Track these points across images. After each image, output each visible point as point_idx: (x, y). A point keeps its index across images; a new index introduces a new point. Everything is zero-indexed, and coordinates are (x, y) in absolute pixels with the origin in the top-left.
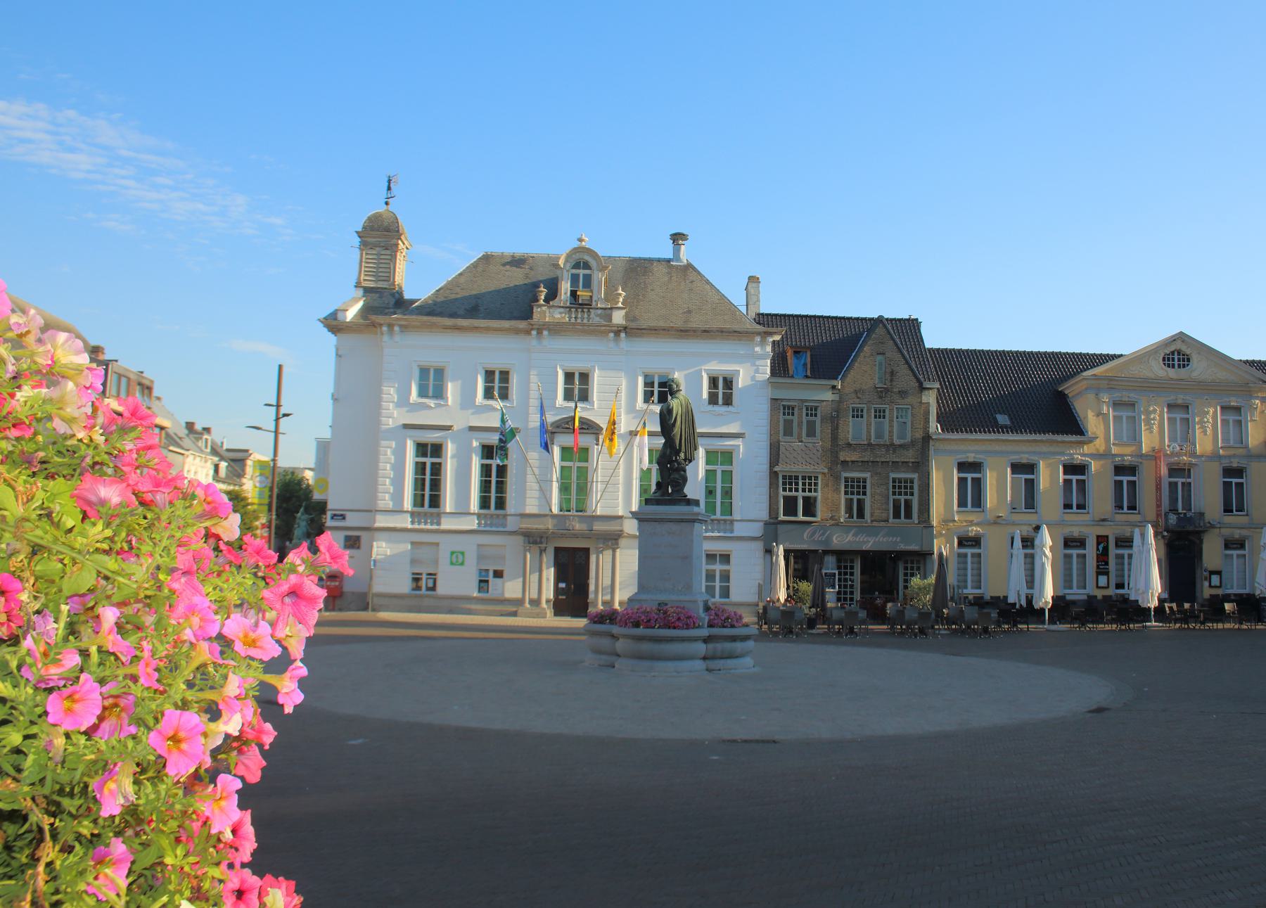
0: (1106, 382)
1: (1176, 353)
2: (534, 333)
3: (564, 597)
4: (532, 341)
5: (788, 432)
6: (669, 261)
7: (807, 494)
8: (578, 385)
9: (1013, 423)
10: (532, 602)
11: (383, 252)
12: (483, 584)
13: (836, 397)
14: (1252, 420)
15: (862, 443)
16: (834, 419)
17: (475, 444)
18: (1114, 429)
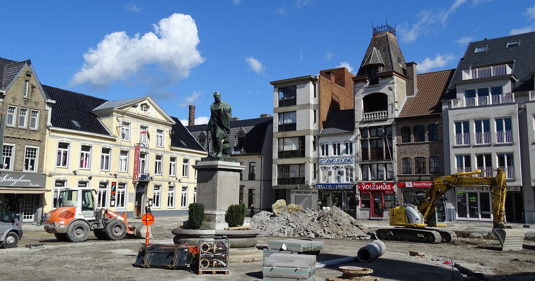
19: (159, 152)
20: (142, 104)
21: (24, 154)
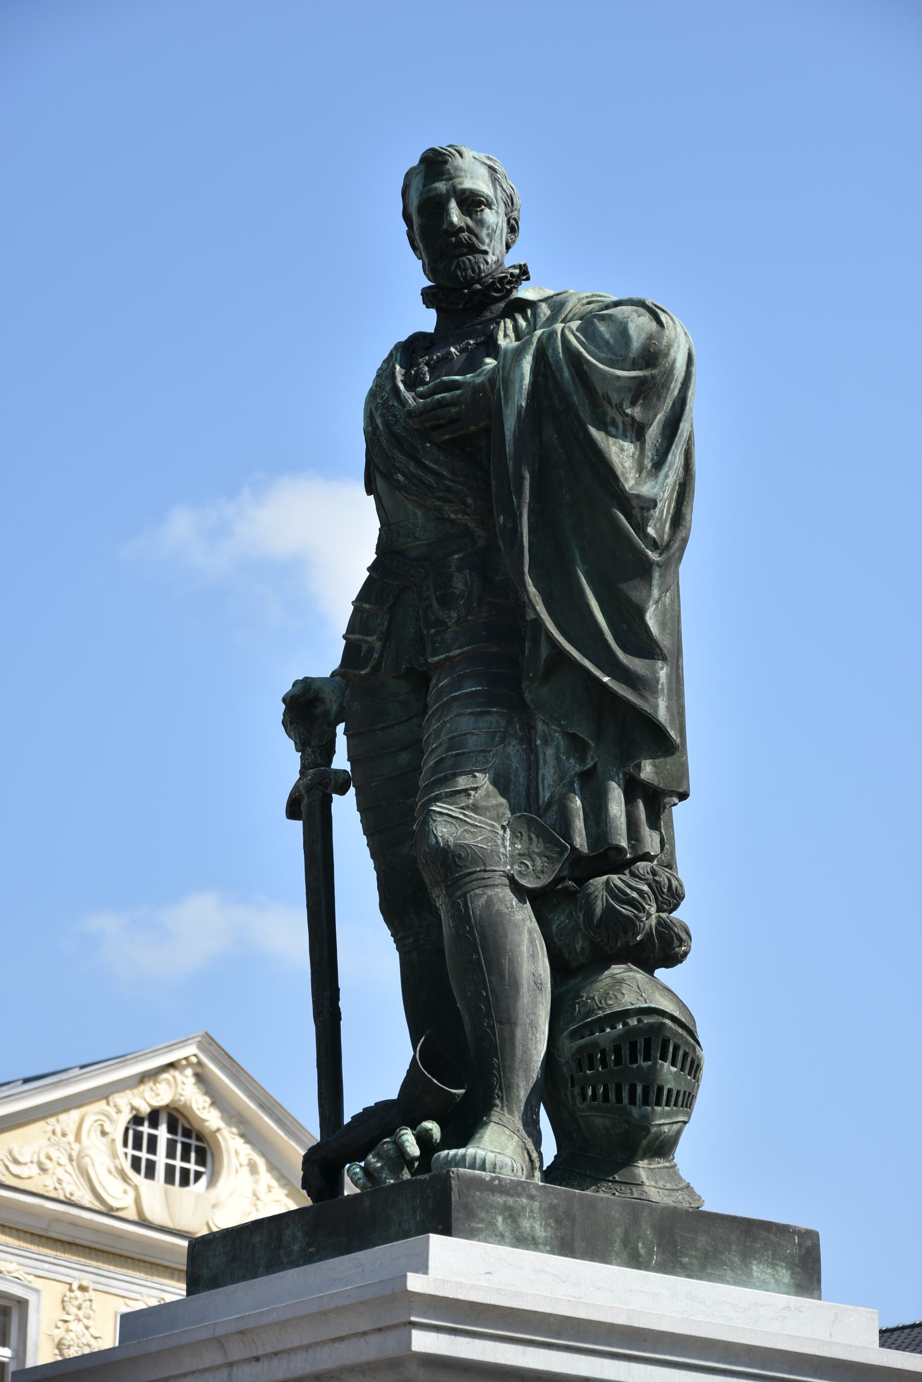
20: (137, 1120)
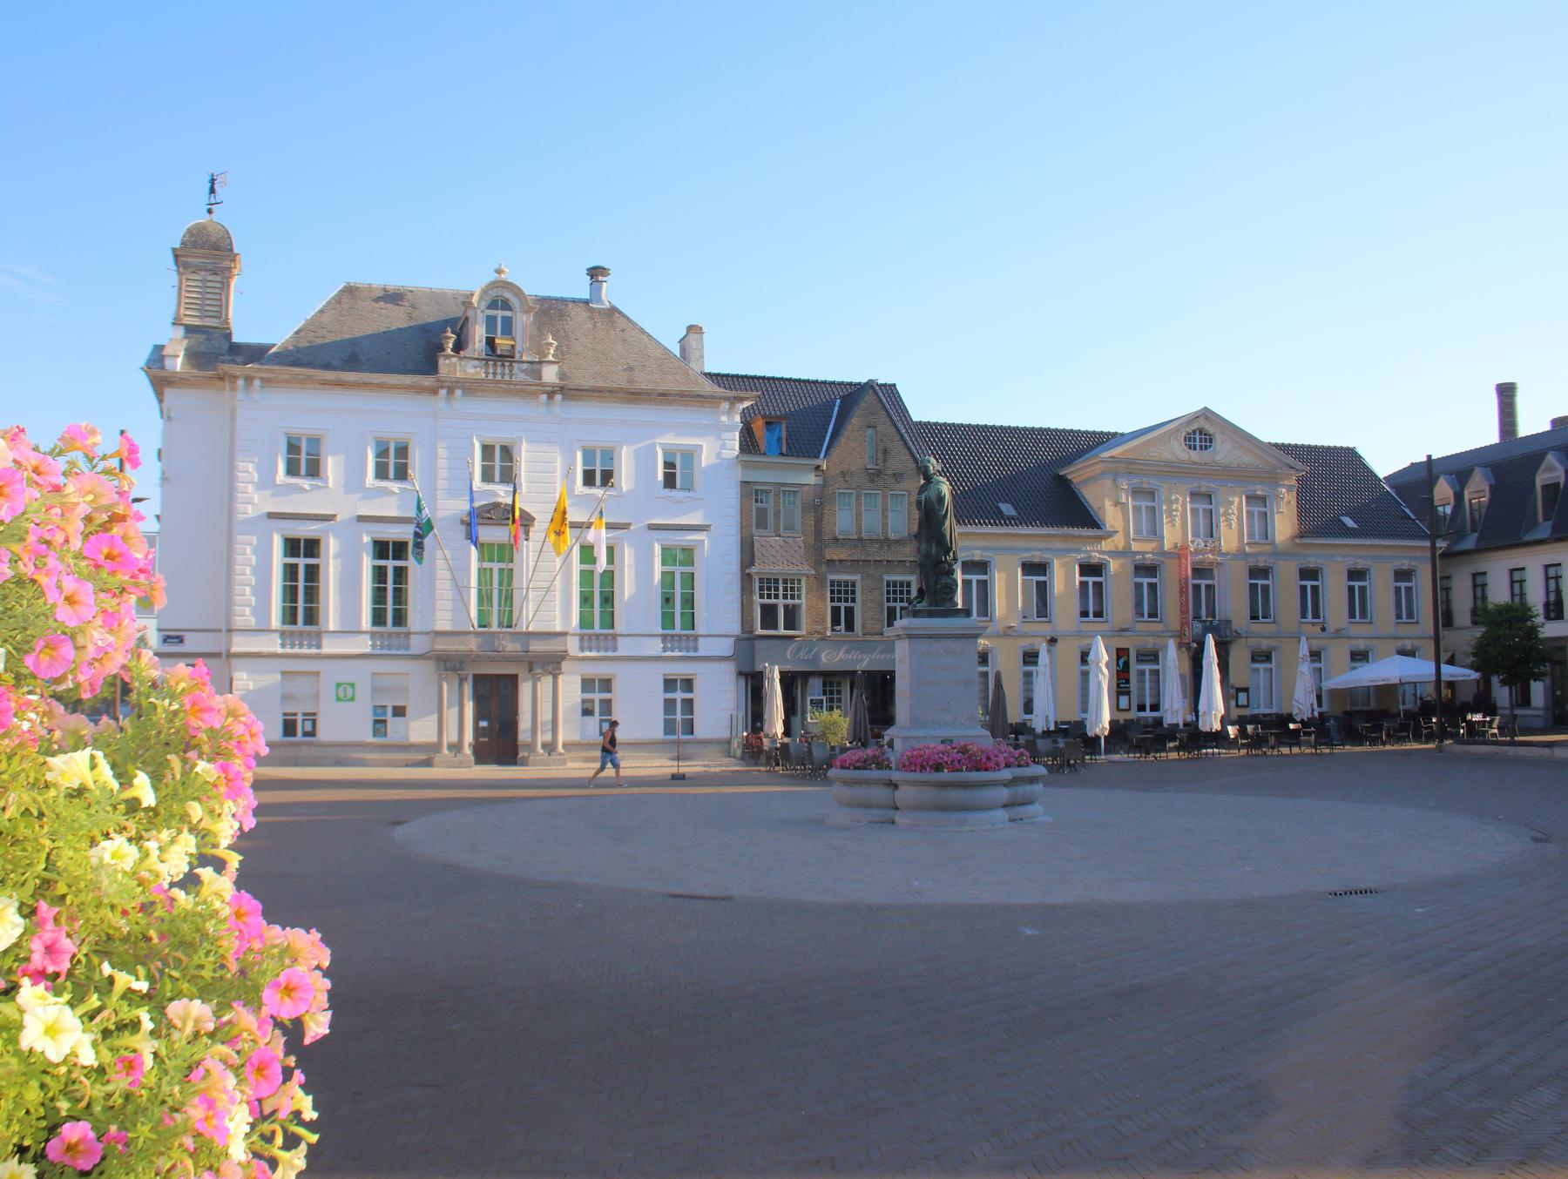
0: (1124, 466)
1: (1197, 432)
2: (443, 392)
3: (486, 739)
4: (440, 400)
5: (762, 523)
6: (586, 302)
7: (789, 601)
8: (499, 459)
9: (1019, 513)
10: (451, 747)
11: (210, 278)
12: (379, 724)
13: (820, 481)
14: (1278, 512)
15: (852, 537)
16: (818, 506)
17: (366, 539)
18: (1134, 518)
19: (1259, 558)
21: (882, 595)
